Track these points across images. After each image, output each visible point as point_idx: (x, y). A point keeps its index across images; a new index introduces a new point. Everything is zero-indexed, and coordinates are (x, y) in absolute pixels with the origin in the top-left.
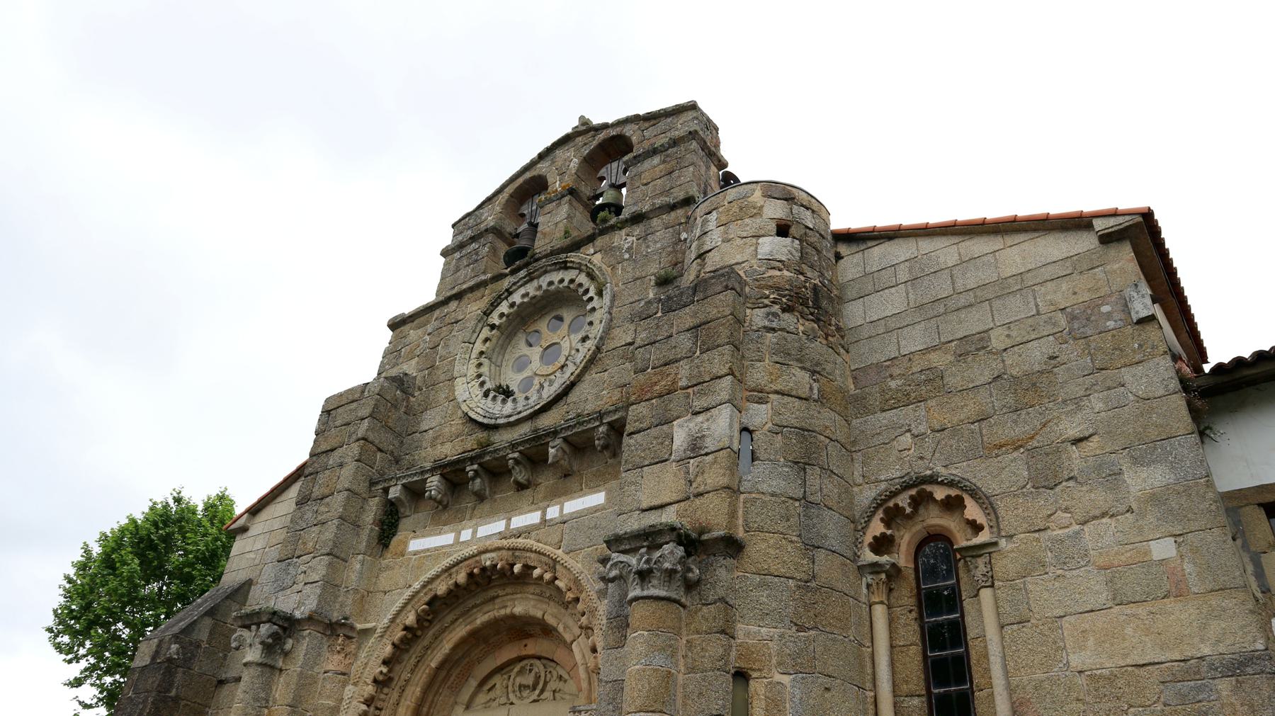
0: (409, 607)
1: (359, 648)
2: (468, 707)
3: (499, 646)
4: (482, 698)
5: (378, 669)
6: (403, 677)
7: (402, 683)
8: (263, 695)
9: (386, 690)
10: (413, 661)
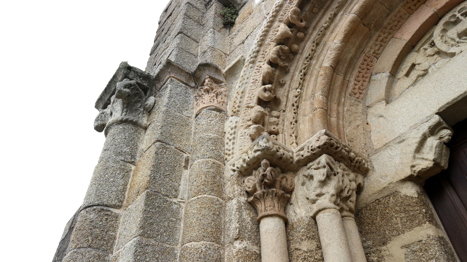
0: (276, 24)
1: (229, 90)
2: (388, 100)
3: (398, 25)
4: (402, 83)
5: (258, 91)
6: (291, 95)
7: (292, 99)
8: (127, 150)
9: (275, 113)
10: (298, 76)
